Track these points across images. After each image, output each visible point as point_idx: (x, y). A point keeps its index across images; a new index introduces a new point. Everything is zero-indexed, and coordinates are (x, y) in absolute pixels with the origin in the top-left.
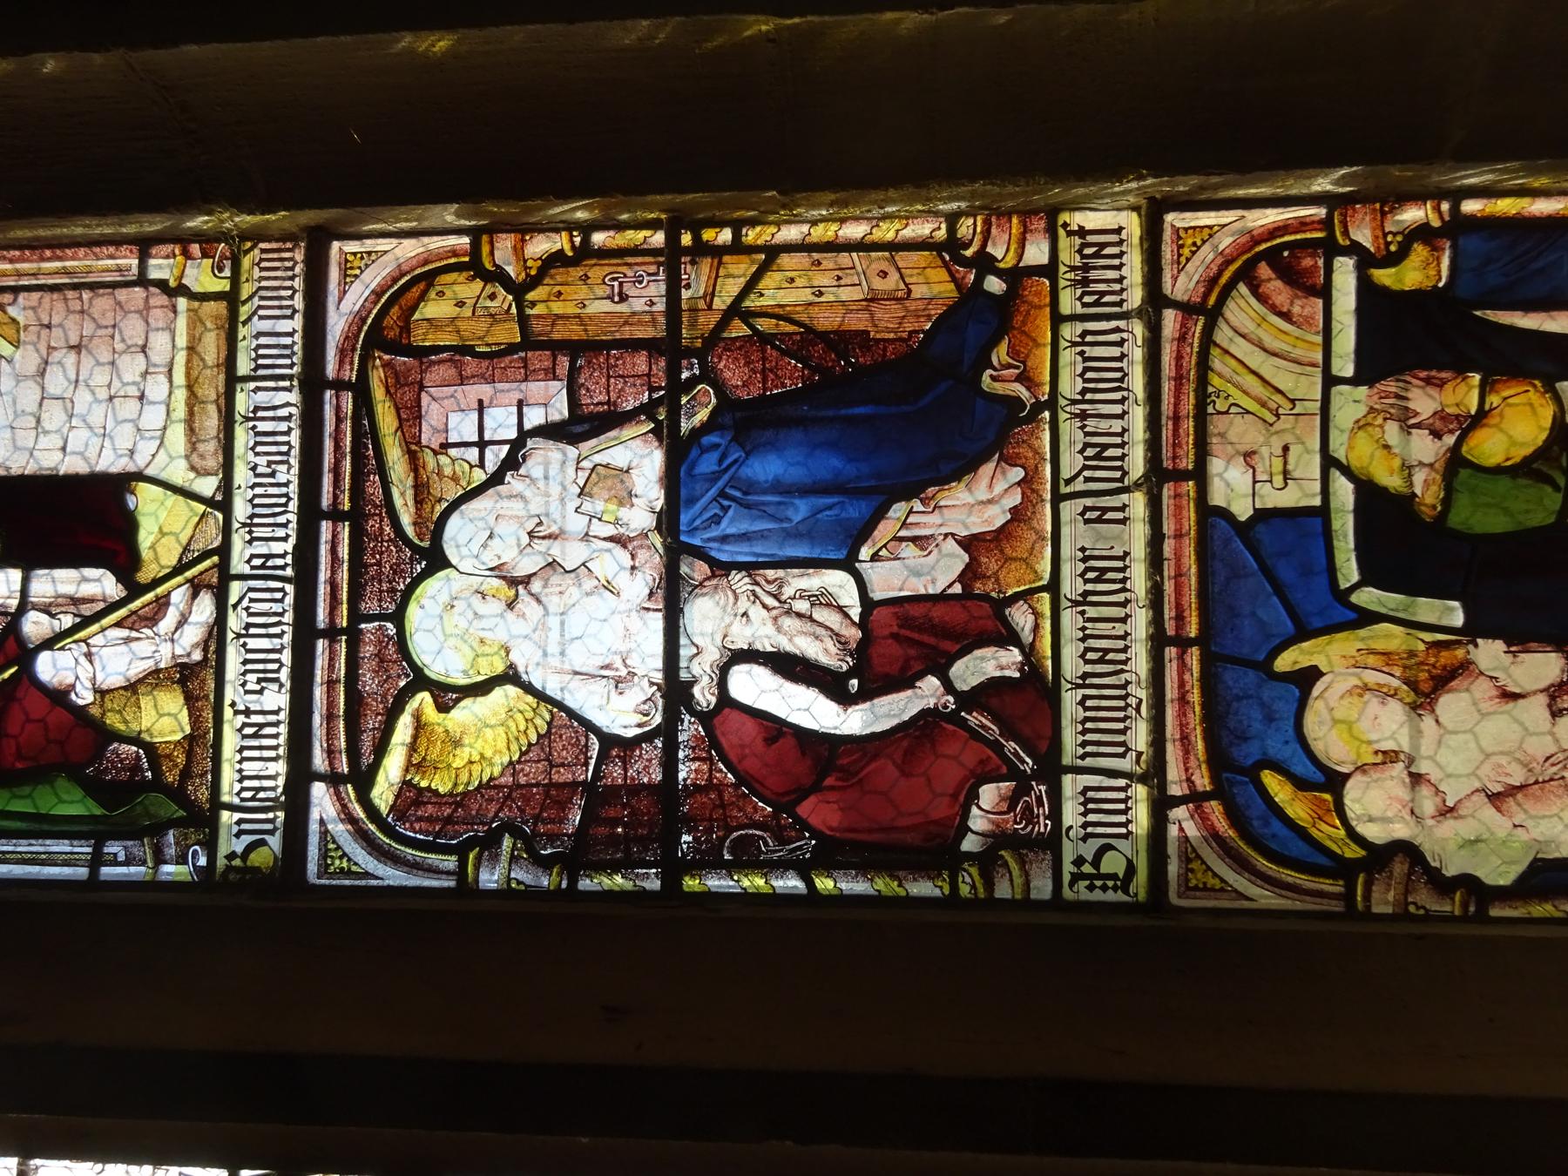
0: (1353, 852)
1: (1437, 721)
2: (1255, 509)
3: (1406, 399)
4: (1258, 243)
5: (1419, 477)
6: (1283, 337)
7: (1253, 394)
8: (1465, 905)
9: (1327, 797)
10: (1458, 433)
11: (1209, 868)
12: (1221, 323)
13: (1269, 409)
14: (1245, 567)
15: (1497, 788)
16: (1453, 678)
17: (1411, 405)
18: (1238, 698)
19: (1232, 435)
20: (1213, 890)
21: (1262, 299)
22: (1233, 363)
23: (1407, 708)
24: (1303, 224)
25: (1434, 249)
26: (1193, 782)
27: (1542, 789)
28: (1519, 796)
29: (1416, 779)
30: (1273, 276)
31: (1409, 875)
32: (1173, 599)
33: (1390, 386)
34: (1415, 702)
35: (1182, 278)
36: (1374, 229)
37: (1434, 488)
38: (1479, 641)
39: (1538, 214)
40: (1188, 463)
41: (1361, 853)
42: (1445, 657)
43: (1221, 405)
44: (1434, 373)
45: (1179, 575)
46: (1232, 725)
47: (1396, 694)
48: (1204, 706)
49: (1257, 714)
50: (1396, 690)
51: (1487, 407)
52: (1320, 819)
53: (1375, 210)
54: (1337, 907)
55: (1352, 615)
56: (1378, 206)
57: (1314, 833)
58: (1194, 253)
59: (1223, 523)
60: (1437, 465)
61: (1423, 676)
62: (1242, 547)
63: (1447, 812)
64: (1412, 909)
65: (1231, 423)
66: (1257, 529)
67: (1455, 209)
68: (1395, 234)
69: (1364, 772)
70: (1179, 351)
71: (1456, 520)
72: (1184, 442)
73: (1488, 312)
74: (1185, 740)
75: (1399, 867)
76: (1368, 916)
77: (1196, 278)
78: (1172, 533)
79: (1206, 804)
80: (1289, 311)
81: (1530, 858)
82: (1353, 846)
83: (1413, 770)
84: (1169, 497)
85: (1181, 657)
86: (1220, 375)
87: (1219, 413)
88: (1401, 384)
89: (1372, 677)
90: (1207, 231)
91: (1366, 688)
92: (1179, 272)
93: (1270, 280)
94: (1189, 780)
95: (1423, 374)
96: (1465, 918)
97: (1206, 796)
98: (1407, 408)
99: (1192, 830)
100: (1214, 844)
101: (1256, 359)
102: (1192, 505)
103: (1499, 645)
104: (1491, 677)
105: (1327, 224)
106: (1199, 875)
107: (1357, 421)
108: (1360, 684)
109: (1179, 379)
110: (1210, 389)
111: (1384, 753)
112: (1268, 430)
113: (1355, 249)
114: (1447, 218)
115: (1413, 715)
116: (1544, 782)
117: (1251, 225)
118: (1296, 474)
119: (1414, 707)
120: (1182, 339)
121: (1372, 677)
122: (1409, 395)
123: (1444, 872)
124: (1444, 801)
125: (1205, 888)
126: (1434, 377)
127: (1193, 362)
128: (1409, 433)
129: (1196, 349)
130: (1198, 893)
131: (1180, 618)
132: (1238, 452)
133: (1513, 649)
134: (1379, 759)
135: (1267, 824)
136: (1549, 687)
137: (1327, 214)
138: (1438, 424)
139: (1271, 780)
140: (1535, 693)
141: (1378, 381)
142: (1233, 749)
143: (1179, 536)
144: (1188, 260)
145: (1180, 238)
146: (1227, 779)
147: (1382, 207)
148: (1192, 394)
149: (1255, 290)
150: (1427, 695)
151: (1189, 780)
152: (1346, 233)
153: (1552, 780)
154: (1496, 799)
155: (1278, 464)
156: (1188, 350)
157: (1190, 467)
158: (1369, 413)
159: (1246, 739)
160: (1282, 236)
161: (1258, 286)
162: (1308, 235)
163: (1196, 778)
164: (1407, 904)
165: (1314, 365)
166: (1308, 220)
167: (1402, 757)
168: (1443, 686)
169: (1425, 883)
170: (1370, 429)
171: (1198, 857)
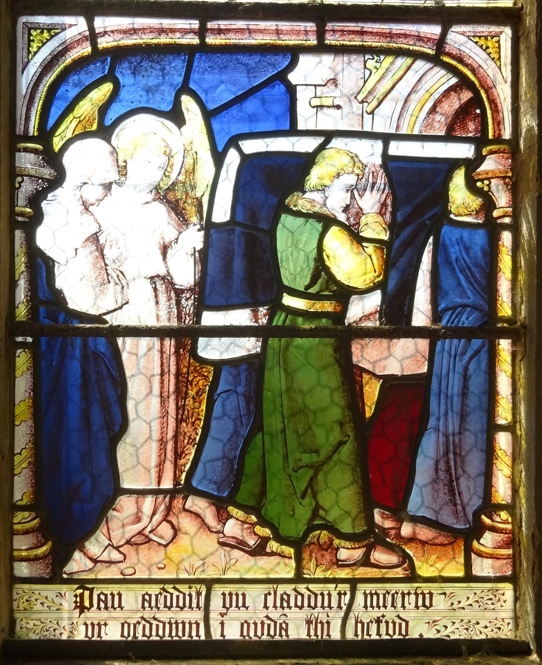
0: (57, 143)
1: (147, 203)
2: (296, 85)
3: (372, 190)
4: (487, 92)
5: (317, 196)
6: (418, 108)
7: (378, 86)
8: (22, 214)
9: (95, 127)
10: (347, 223)
11: (44, 44)
12: (429, 65)
13: (367, 96)
14: (255, 77)
15: (102, 239)
16: (177, 215)
17: (368, 193)
18: (163, 70)
19: (349, 70)
20: (29, 46)
21: (446, 93)
22: (400, 73)
23: (156, 183)
24: (498, 123)
25: (477, 212)
26: (104, 35)
27: (101, 268)
28: (97, 254)
29: (108, 187)
30: (462, 102)
31: (42, 179)
32: (233, 27)
33: (381, 180)
34: (161, 189)
35: (463, 39)
36: (493, 171)
37: (309, 206)
38: (202, 233)
39: (499, 283)
40: (330, 40)
41: (57, 148)
42: (191, 210)
43: (371, 64)
44: (390, 209)
45: (250, 31)
46: (144, 64)
47: (166, 176)
48: (157, 45)
49: (152, 82)
50: (169, 176)
51: (364, 244)
52: (80, 122)
53: (507, 172)
54: (20, 129)
55: (220, 148)
56: (510, 174)
57: (71, 117)
58: (481, 47)
59: (286, 63)
60: (325, 209)
61: (179, 195)
62: (269, 75)
63: (85, 206)
64: (19, 179)
65: (358, 70)
66: (282, 86)
67: (505, 227)
68: (489, 185)
69: (112, 153)
70: (410, 36)
71: (286, 220)
72: (345, 38)
73: (431, 247)
74: (134, 31)
75: (47, 172)
76: (13, 150)
77: (462, 48)
78: (280, 27)
79: (88, 43)
80: (437, 112)
81: (54, 258)
82: (61, 143)
83: (114, 185)
84: (306, 27)
85: (192, 31)
86: (392, 63)
87: (365, 62)
88: (382, 187)
89: (177, 161)
90: (496, 56)
91: (170, 157)
92: (468, 36)
93: (460, 99)
94: (105, 33)
95: (389, 202)
96: (12, 213)
97: (94, 44)
98: (365, 190)
99: (69, 34)
100: (60, 48)
101: (403, 88)
102: (300, 42)
103: (200, 246)
104: (177, 239)
105: (498, 140)
106: (39, 37)
107: (357, 156)
108: (172, 153)
109: (390, 36)
110: (382, 57)
111: (125, 167)
112: (352, 95)
113: (479, 159)
114: (499, 221)
115: (152, 187)
116: (106, 270)
117: (499, 87)
118: (320, 113)
119: (157, 188)
120: (419, 38)
121: (177, 161)
122: (375, 192)
123: (45, 202)
124: (92, 205)
125: (30, 41)
126: (386, 209)
127: (402, 46)
128: (347, 191)
129: (411, 48)
130: (26, 36)
131: (219, 31)
132: (336, 74)
133: (197, 254)
134: (121, 164)
135: (76, 85)
136: (170, 276)
137: (505, 140)
138: (353, 211)
139: (107, 88)
140: (166, 267)
141: (385, 171)
142: (126, 64)
143: (278, 32)
144: (476, 43)
145: (492, 37)
146: (107, 59)
147: (508, 177)
148: (379, 44)
149: (452, 89)
150: (165, 197)
151: (105, 33)
152: (491, 153)
153: (108, 275)
154: (95, 238)
155: (327, 102)
156: (411, 43)
157: (327, 42)
158: (362, 164)
159: (134, 73)
160: (491, 109)
161: (455, 91)
162: (490, 127)
163: (107, 38)
164: (22, 176)
165: (398, 128)
166: (502, 127)
167: (123, 179)
168: (171, 207)
169: (36, 189)
170: (351, 165)
171: (52, 37)
